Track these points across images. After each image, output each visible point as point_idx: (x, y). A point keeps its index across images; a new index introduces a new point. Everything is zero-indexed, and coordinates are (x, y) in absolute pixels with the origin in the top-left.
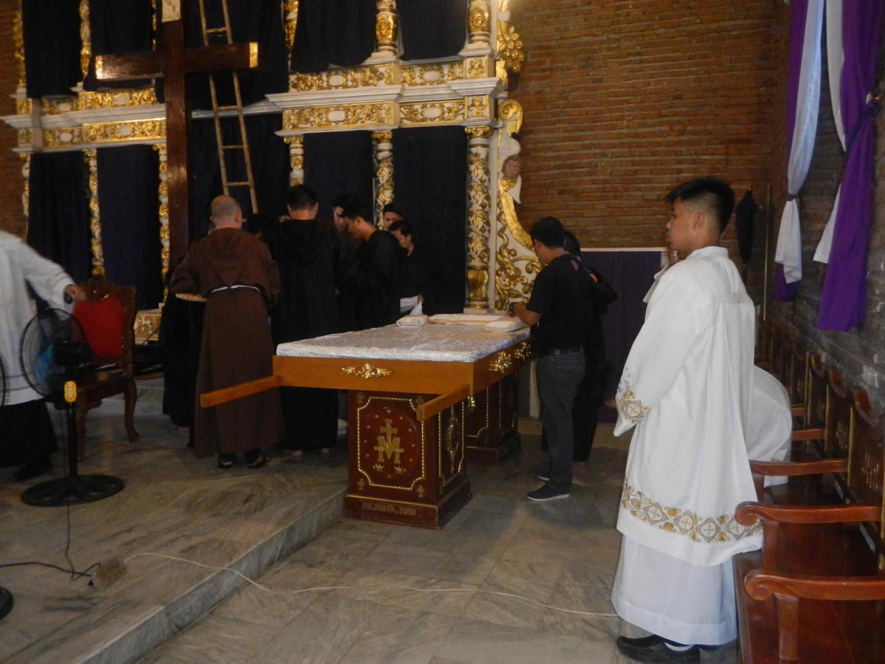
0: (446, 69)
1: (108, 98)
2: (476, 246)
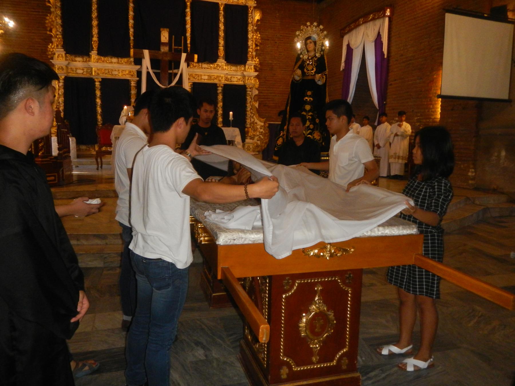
0: (239, 67)
1: (106, 59)
2: (248, 121)
